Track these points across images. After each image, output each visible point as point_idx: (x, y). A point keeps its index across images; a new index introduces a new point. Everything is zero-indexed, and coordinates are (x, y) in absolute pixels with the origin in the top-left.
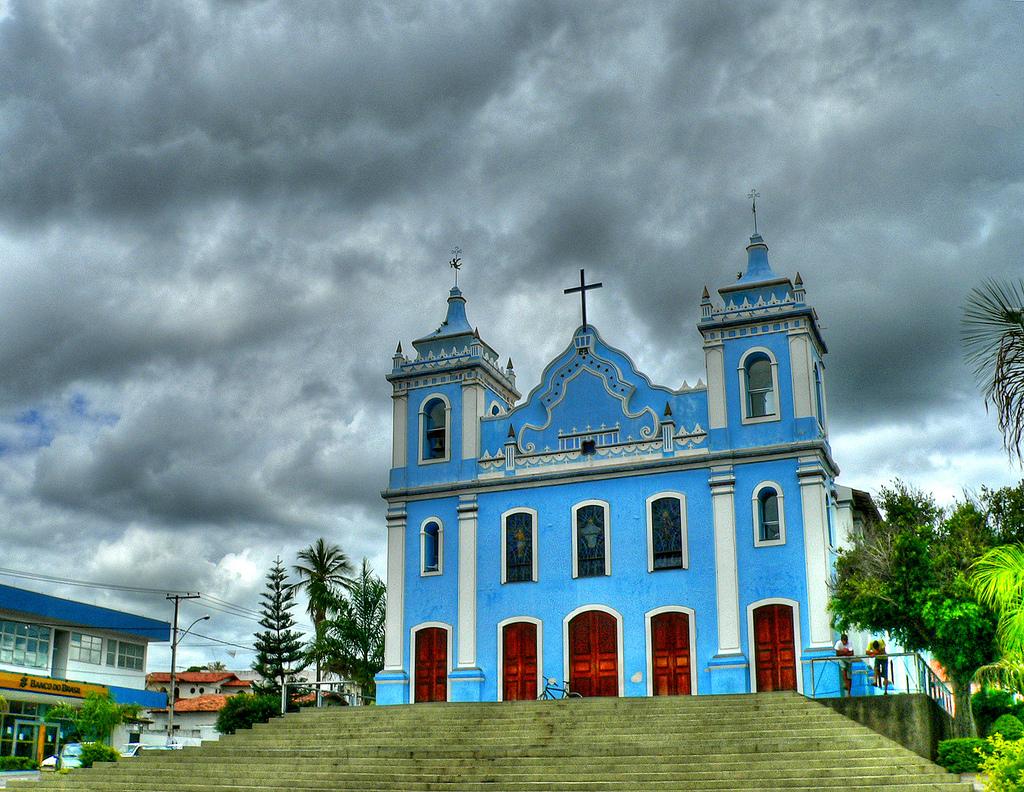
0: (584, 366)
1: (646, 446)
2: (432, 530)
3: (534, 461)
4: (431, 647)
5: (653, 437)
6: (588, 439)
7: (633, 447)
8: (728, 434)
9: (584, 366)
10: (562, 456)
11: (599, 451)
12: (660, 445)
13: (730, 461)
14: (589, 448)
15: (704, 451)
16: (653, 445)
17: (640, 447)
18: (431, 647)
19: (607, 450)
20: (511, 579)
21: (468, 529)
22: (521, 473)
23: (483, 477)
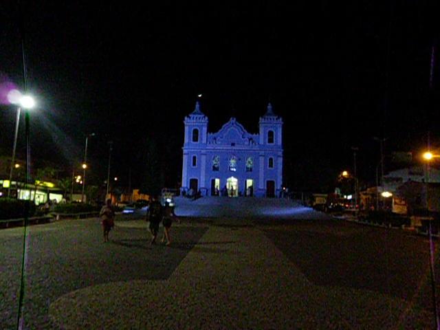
2: (194, 158)
4: (194, 183)
8: (264, 145)
11: (236, 145)
14: (233, 144)
18: (194, 183)
21: (203, 158)
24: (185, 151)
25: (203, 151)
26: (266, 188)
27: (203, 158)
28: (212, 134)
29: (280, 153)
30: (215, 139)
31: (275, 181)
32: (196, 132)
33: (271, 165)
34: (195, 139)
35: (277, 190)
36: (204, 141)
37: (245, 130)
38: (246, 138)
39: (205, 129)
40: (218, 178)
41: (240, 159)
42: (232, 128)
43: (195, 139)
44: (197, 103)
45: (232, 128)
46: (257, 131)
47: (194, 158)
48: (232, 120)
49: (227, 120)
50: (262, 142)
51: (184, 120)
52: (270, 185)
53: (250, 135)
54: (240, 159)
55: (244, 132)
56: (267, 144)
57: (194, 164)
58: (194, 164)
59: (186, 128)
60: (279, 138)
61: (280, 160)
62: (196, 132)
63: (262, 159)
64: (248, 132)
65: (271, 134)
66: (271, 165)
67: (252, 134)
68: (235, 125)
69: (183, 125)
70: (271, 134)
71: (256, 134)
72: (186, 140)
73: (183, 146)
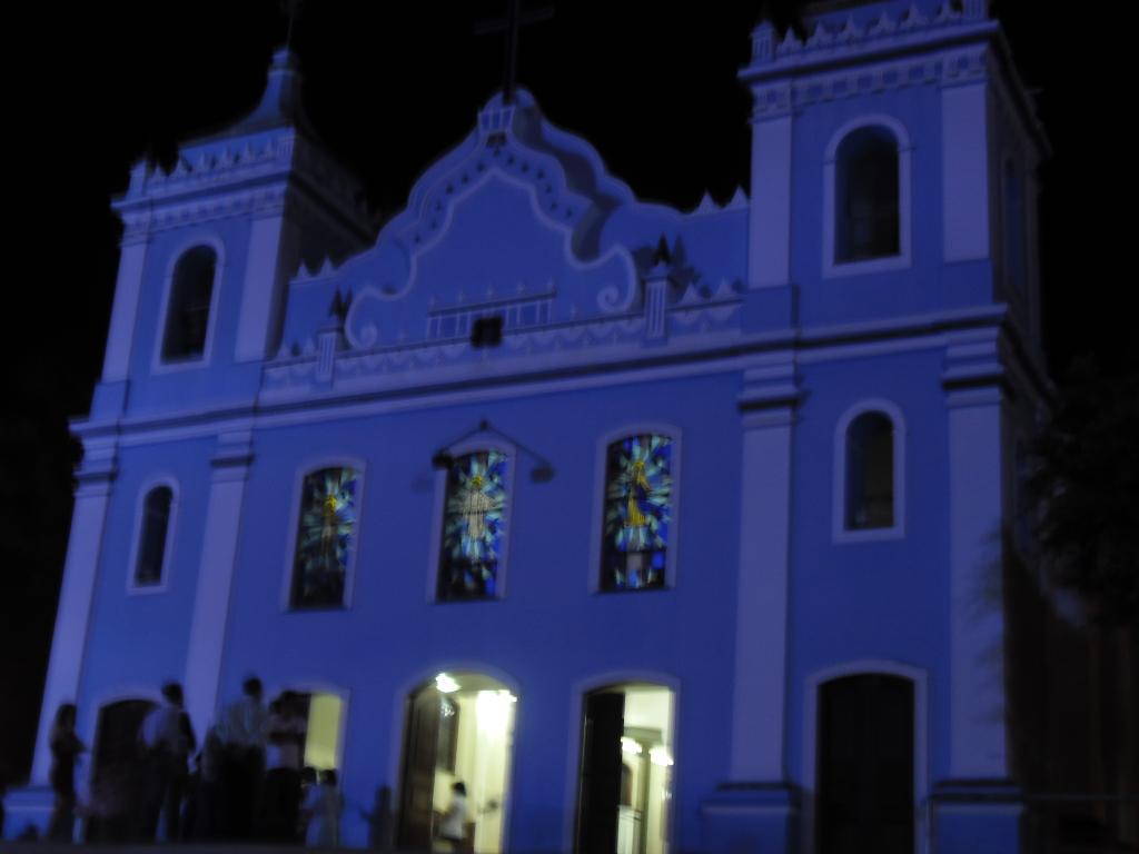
0: (495, 171)
1: (609, 326)
2: (160, 499)
3: (379, 358)
5: (625, 307)
6: (486, 313)
7: (579, 329)
9: (495, 171)
10: (432, 351)
11: (510, 340)
12: (639, 323)
13: (788, 356)
14: (487, 332)
15: (735, 337)
16: (623, 324)
17: (596, 328)
19: (524, 337)
20: (300, 601)
22: (344, 387)
23: (269, 396)
24: (97, 451)
25: (235, 432)
26: (808, 779)
27: (227, 492)
28: (327, 268)
29: (979, 349)
30: (340, 308)
31: (919, 676)
32: (196, 274)
33: (869, 496)
34: (185, 337)
35: (953, 790)
36: (251, 340)
37: (619, 188)
38: (617, 251)
39: (267, 236)
40: (336, 682)
41: (542, 474)
42: (508, 178)
43: (185, 337)
44: (281, 56)
45: (508, 178)
46: (727, 171)
47: (160, 499)
48: (499, 115)
49: (457, 127)
50: (768, 265)
51: (122, 185)
52: (864, 725)
53: (663, 215)
54: (542, 474)
55: (607, 204)
56: (830, 269)
57: (151, 565)
58: (151, 565)
59: (132, 259)
60: (961, 192)
61: (977, 440)
62: (196, 274)
63: (766, 447)
64: (645, 192)
65: (870, 171)
66: (869, 496)
67: (686, 203)
68: (515, 146)
69: (116, 228)
70: (870, 171)
71: (722, 198)
72: (117, 363)
73: (83, 408)
